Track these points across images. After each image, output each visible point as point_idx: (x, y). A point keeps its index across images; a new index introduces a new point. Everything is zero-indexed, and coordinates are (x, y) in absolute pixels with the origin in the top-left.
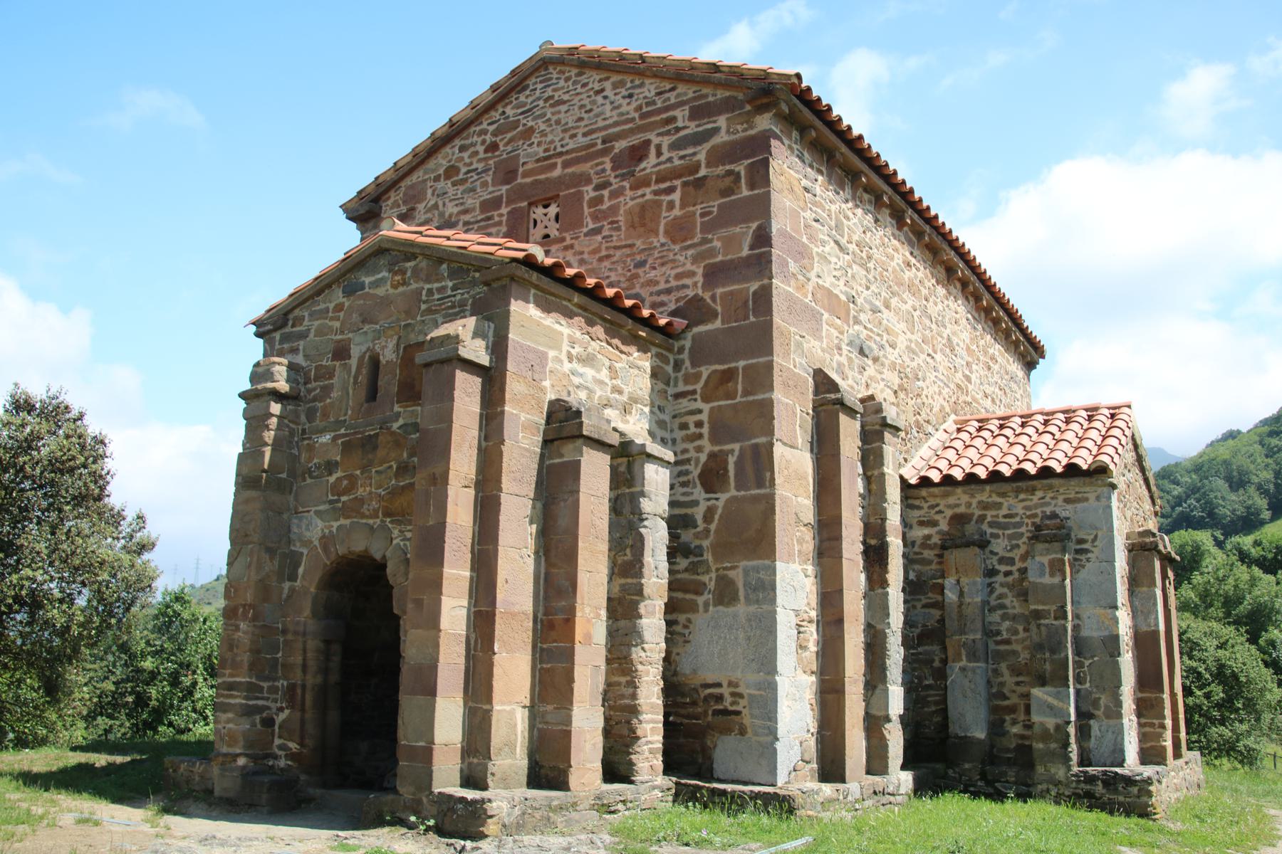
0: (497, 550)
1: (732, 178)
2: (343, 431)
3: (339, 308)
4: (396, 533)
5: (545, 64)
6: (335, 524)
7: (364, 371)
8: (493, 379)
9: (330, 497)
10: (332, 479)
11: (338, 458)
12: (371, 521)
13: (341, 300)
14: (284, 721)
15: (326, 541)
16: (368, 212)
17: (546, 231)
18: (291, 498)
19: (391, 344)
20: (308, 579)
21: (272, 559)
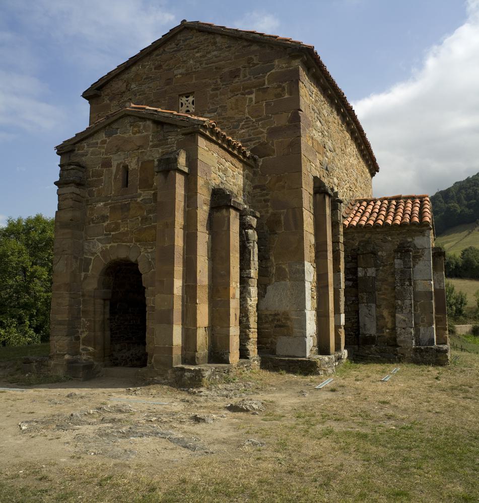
0: (196, 257)
1: (280, 89)
2: (110, 201)
3: (104, 142)
4: (142, 250)
5: (185, 28)
6: (109, 245)
7: (120, 173)
8: (191, 179)
9: (105, 232)
10: (105, 224)
11: (108, 214)
12: (128, 244)
13: (105, 138)
14: (85, 337)
15: (104, 253)
16: (95, 94)
18: (83, 233)
19: (135, 161)
20: (95, 271)
21: (76, 262)
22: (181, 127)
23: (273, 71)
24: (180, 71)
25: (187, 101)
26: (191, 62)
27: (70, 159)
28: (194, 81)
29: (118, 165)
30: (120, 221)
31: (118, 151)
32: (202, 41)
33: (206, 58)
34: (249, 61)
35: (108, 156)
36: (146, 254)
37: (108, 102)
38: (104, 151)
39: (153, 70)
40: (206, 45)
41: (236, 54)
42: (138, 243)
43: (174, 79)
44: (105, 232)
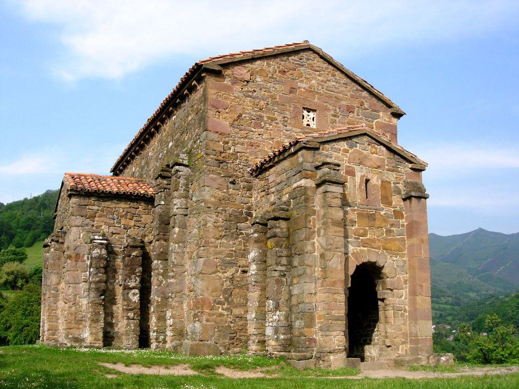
2: (356, 208)
3: (347, 151)
4: (389, 257)
6: (359, 248)
12: (377, 250)
17: (308, 123)
19: (376, 177)
22: (411, 162)
23: (379, 120)
24: (304, 85)
25: (308, 116)
26: (313, 82)
27: (314, 156)
28: (316, 100)
29: (362, 177)
30: (367, 228)
31: (360, 164)
32: (323, 68)
33: (326, 85)
34: (362, 104)
35: (350, 165)
36: (392, 262)
37: (230, 83)
38: (347, 159)
39: (277, 73)
40: (327, 73)
41: (351, 93)
42: (385, 251)
43: (298, 90)
44: (354, 236)
